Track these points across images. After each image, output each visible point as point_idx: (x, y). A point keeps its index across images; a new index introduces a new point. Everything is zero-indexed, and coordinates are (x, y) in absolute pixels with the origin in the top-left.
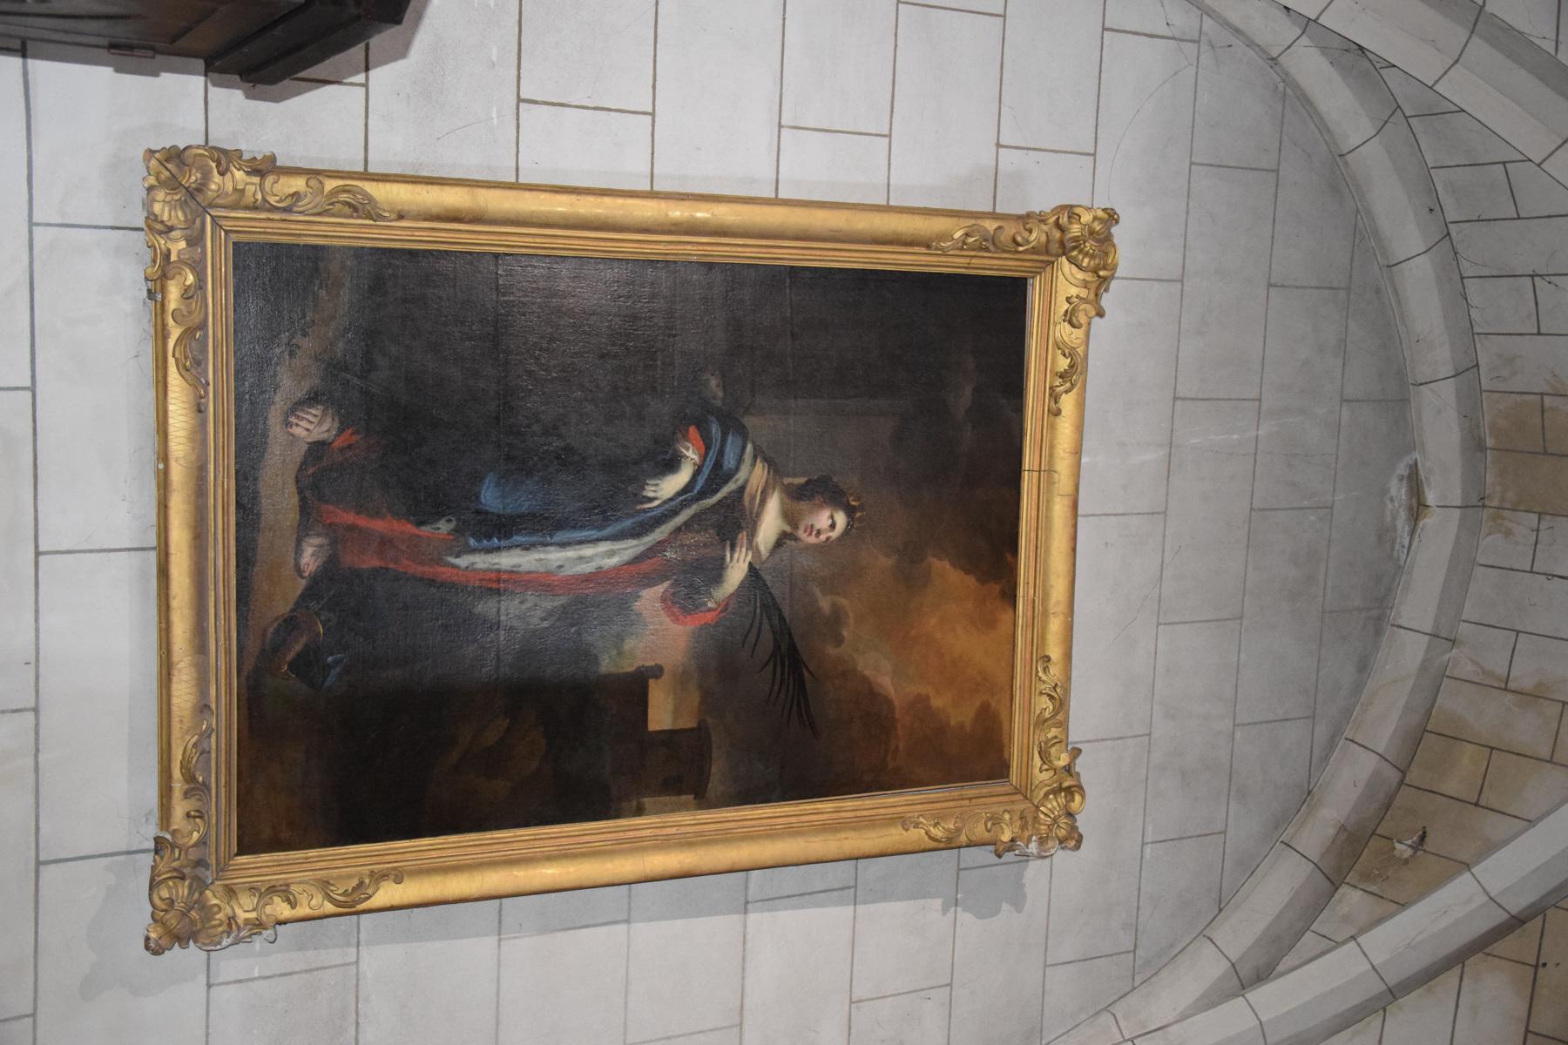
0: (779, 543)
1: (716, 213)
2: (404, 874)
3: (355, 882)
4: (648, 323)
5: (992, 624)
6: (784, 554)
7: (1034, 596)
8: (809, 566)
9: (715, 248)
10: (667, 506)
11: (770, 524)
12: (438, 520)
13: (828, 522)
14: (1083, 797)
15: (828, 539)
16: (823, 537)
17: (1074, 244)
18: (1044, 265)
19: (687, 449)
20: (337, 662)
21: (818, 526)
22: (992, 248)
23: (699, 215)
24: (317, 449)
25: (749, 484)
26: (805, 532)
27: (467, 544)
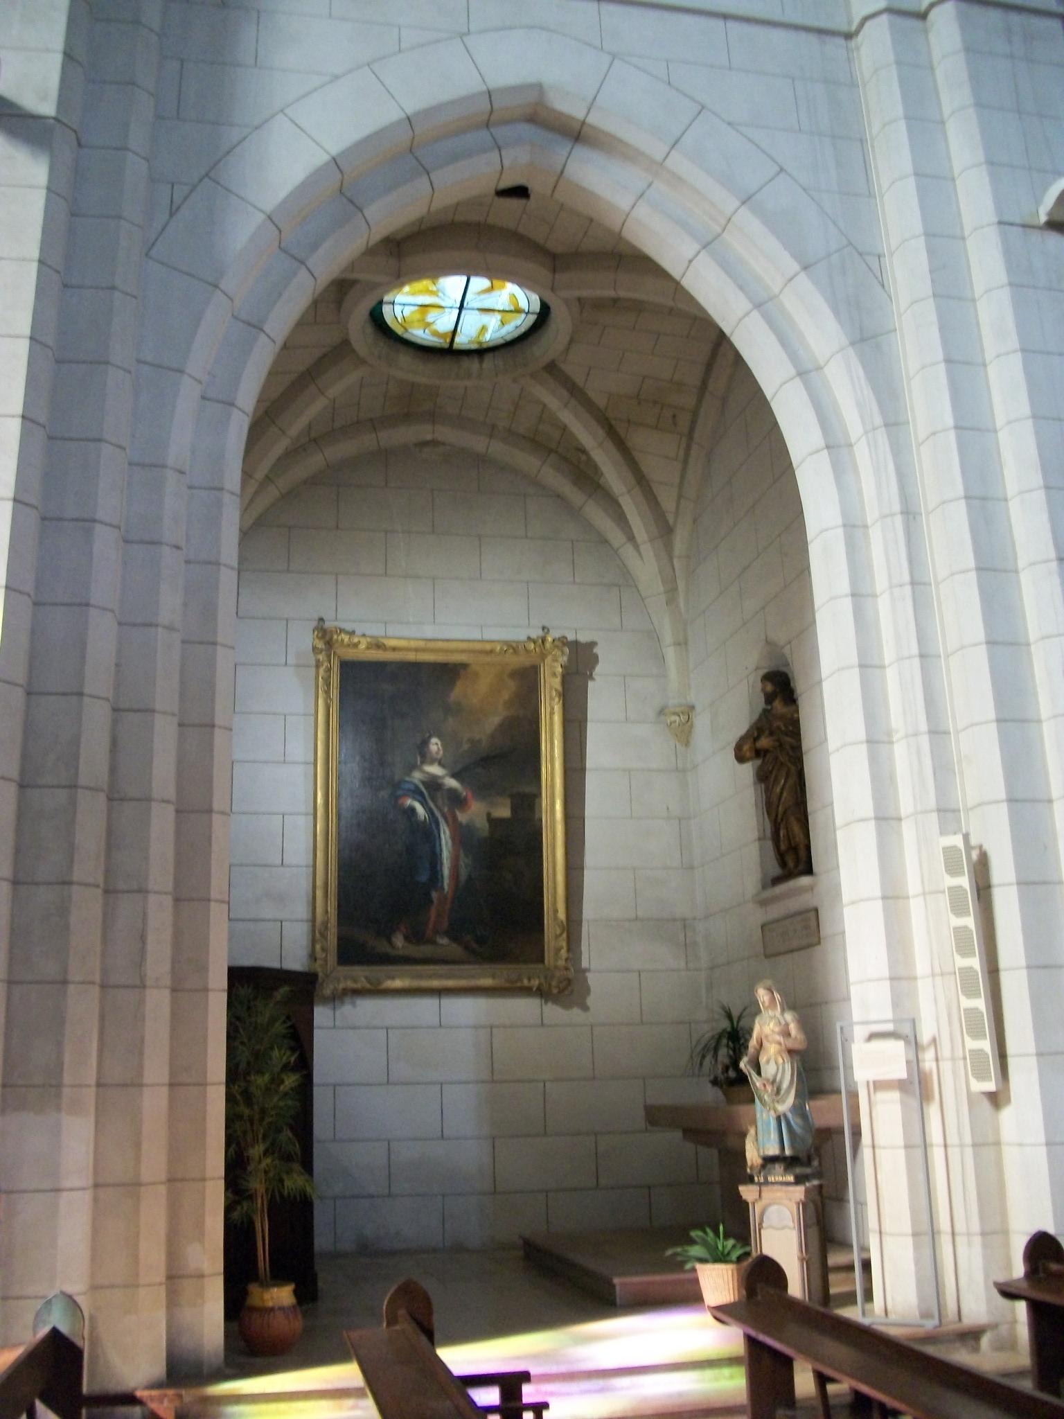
11: (435, 770)
13: (435, 745)
24: (406, 938)
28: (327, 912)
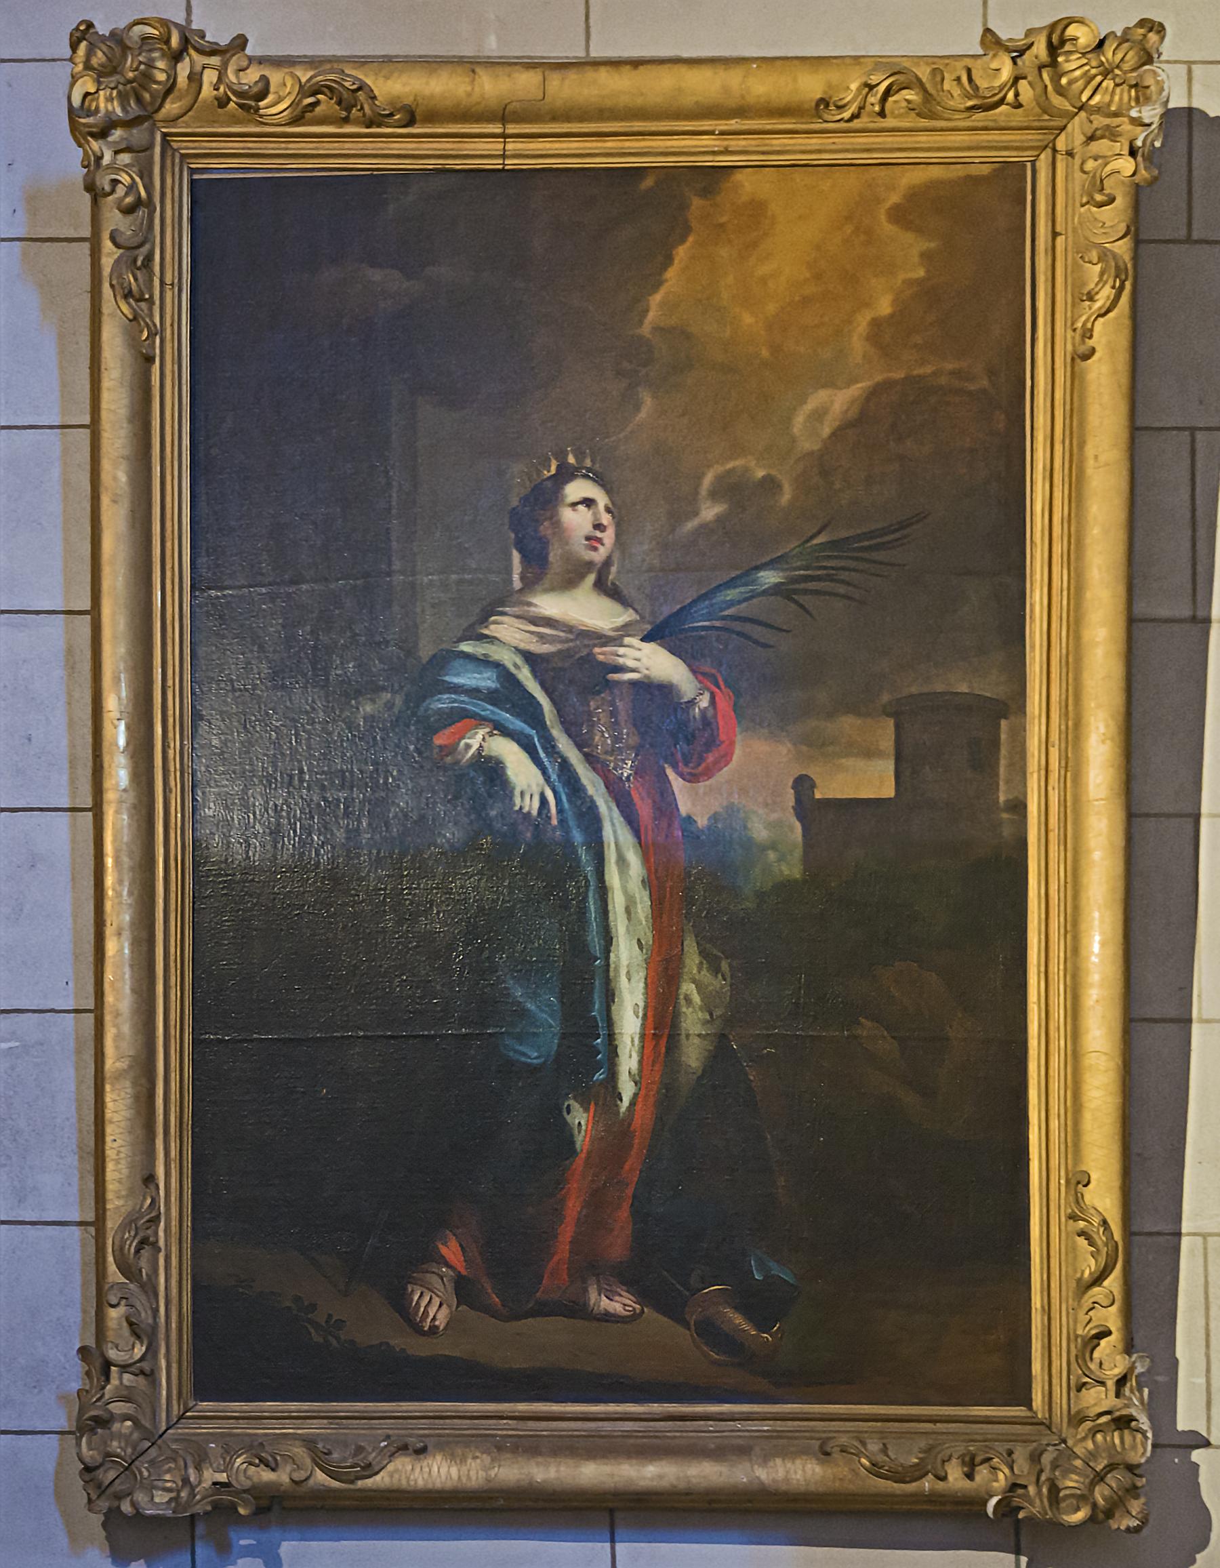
0: (614, 593)
1: (117, 715)
2: (1079, 1169)
3: (1082, 1242)
4: (284, 814)
5: (756, 210)
6: (628, 591)
7: (711, 133)
8: (651, 542)
9: (170, 712)
10: (554, 777)
12: (566, 1123)
14: (1070, 21)
15: (608, 510)
16: (606, 519)
17: (132, 102)
18: (169, 153)
19: (468, 746)
20: (762, 1266)
21: (587, 528)
22: (145, 250)
23: (122, 742)
25: (522, 646)
26: (595, 549)
27: (601, 1083)
28: (149, 1179)
